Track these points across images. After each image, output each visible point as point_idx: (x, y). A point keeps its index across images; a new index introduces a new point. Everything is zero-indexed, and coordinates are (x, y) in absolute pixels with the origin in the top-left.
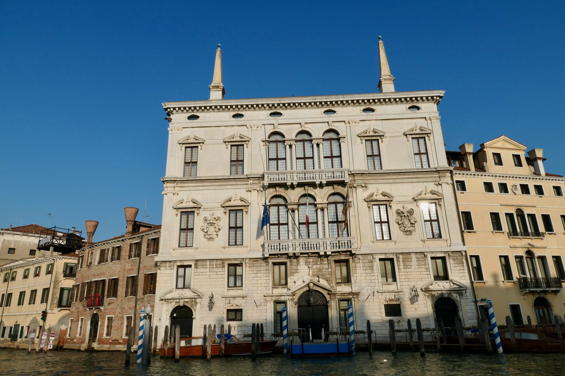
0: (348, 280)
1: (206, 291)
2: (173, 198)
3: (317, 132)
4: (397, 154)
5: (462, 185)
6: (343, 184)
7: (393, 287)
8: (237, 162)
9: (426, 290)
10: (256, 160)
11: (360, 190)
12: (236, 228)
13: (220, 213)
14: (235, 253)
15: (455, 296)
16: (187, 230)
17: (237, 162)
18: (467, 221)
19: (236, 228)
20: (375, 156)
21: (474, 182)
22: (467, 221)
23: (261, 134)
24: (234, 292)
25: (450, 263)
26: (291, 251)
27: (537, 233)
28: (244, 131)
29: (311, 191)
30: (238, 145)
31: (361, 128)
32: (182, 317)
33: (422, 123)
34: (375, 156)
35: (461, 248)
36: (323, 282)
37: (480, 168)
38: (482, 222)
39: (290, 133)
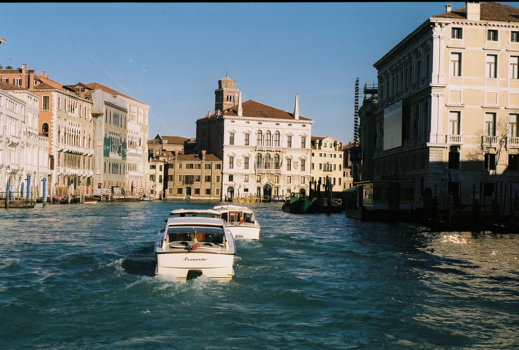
0: (278, 182)
1: (238, 183)
2: (227, 152)
3: (273, 133)
4: (297, 143)
5: (313, 155)
6: (280, 151)
7: (289, 185)
8: (247, 140)
9: (298, 186)
10: (253, 141)
11: (284, 154)
12: (247, 164)
13: (241, 158)
14: (246, 171)
15: (305, 188)
16: (231, 163)
17: (247, 140)
18: (313, 165)
19: (247, 164)
20: (290, 142)
21: (317, 152)
22: (313, 165)
23: (256, 130)
24: (246, 183)
25: (306, 179)
26: (263, 173)
27: (331, 171)
28: (249, 129)
29: (269, 153)
30: (247, 135)
31: (286, 132)
32: (231, 190)
33: (306, 132)
34: (290, 142)
35: (310, 175)
36: (271, 182)
37: (320, 148)
38: (317, 166)
39: (264, 132)
